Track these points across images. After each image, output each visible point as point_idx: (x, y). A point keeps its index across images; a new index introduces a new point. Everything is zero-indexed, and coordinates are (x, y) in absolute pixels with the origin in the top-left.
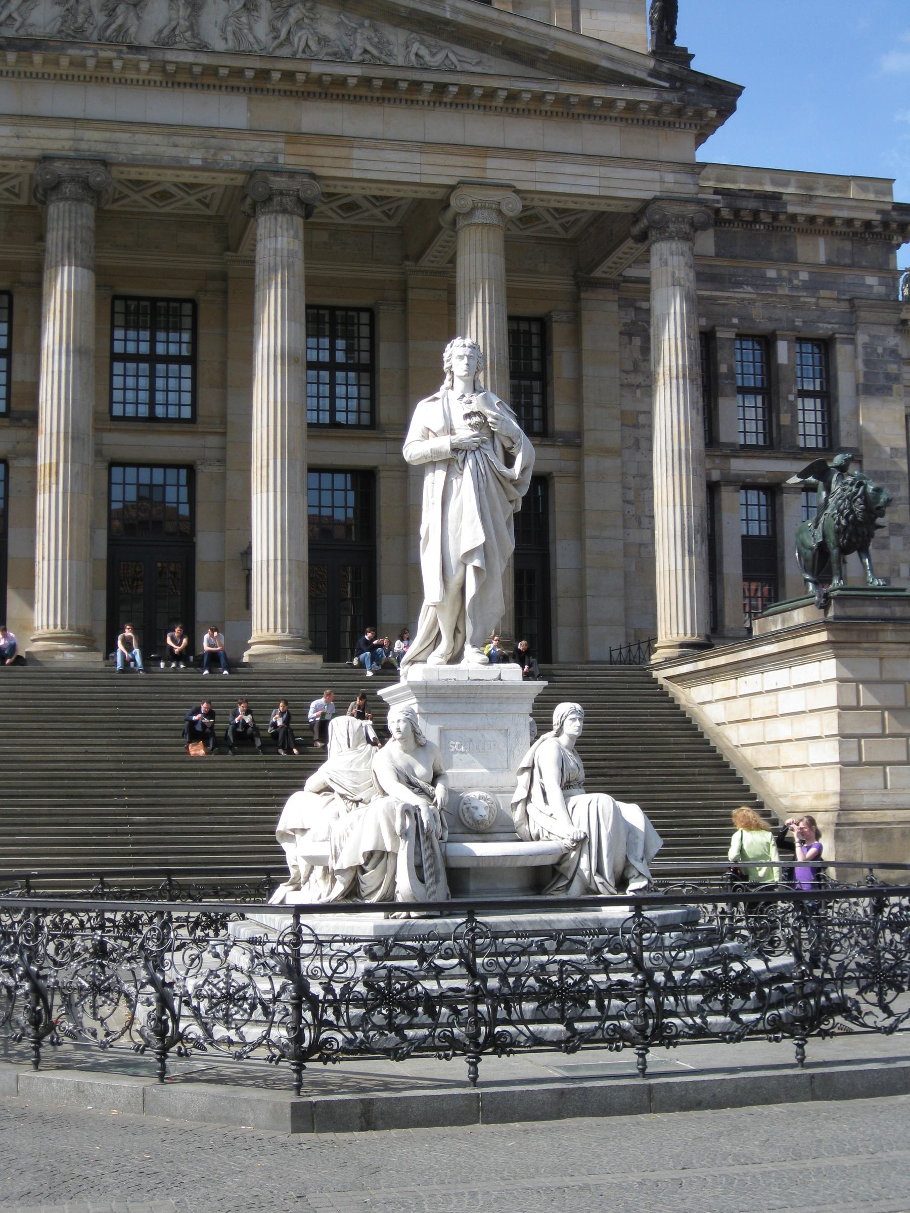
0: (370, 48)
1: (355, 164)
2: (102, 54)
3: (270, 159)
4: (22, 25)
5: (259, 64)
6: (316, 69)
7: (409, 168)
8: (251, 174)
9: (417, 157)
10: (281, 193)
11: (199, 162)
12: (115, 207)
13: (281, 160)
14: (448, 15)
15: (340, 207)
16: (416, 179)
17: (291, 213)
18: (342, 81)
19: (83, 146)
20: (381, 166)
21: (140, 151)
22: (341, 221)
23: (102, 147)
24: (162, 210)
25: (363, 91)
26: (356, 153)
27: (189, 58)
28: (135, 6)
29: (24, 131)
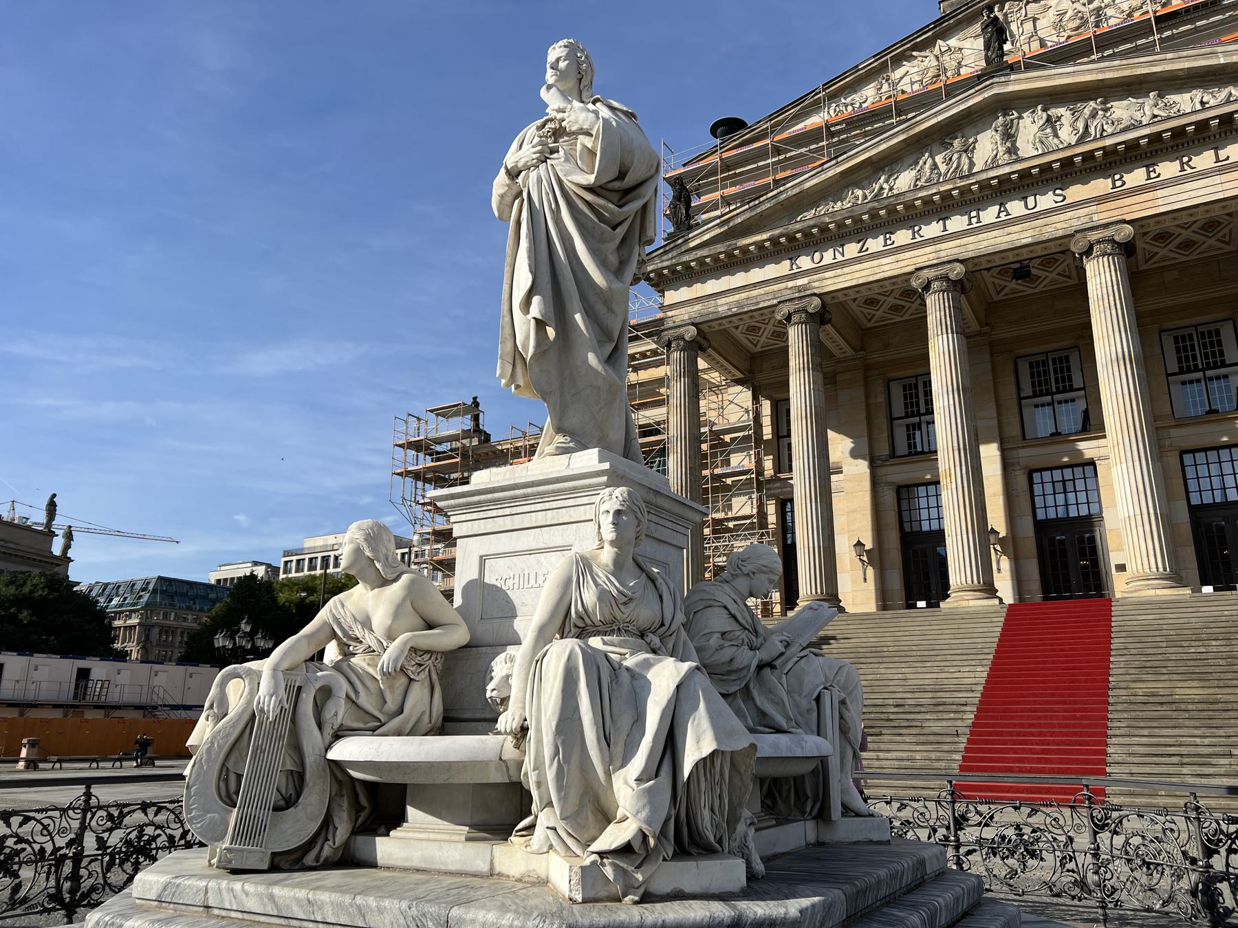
0: (1156, 112)
1: (1160, 202)
2: (942, 189)
3: (1084, 220)
4: (891, 189)
5: (1061, 155)
6: (1109, 142)
7: (1212, 190)
8: (1072, 235)
9: (1217, 179)
10: (1099, 242)
11: (1029, 240)
12: (1000, 297)
13: (1095, 218)
14: (1222, 61)
15: (1178, 247)
16: (1220, 196)
17: (1109, 255)
18: (1132, 145)
19: (943, 254)
20: (1186, 196)
21: (985, 244)
22: (1186, 259)
23: (956, 251)
24: (1037, 290)
25: (1157, 146)
26: (1160, 193)
27: (1007, 170)
28: (965, 151)
29: (901, 256)
